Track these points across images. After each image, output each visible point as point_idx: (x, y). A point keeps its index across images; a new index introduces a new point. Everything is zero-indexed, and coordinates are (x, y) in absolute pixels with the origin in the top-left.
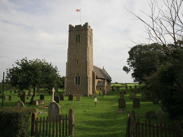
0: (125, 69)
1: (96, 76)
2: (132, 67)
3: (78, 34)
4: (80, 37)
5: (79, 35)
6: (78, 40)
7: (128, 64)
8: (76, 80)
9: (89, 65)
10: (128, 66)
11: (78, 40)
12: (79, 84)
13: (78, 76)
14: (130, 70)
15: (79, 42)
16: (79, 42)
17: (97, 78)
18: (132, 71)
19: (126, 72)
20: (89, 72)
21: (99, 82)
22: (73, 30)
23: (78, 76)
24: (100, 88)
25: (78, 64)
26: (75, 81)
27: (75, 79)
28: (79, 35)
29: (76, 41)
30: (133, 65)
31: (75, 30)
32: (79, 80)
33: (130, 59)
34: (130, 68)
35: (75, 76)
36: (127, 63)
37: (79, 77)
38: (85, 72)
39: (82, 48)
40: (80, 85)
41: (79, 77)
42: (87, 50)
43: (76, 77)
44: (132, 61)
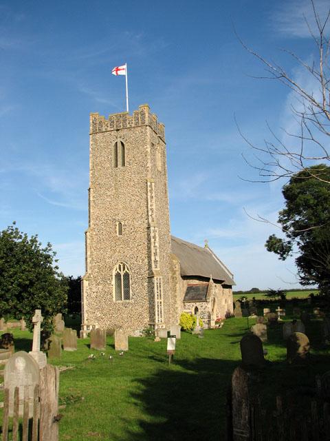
0: (274, 246)
1: (181, 268)
2: (298, 239)
3: (119, 140)
4: (126, 151)
5: (122, 143)
7: (285, 229)
8: (119, 286)
9: (154, 237)
10: (282, 236)
12: (127, 297)
13: (122, 273)
14: (289, 249)
15: (124, 164)
16: (124, 164)
17: (185, 277)
18: (296, 252)
19: (279, 256)
20: (158, 259)
21: (190, 289)
22: (104, 130)
23: (122, 273)
24: (196, 309)
25: (120, 232)
26: (114, 287)
27: (113, 282)
28: (122, 143)
29: (113, 161)
30: (299, 229)
31: (109, 129)
32: (127, 286)
33: (288, 213)
34: (289, 243)
35: (114, 273)
36: (280, 225)
37: (126, 275)
39: (132, 184)
43: (118, 276)
44: (297, 218)
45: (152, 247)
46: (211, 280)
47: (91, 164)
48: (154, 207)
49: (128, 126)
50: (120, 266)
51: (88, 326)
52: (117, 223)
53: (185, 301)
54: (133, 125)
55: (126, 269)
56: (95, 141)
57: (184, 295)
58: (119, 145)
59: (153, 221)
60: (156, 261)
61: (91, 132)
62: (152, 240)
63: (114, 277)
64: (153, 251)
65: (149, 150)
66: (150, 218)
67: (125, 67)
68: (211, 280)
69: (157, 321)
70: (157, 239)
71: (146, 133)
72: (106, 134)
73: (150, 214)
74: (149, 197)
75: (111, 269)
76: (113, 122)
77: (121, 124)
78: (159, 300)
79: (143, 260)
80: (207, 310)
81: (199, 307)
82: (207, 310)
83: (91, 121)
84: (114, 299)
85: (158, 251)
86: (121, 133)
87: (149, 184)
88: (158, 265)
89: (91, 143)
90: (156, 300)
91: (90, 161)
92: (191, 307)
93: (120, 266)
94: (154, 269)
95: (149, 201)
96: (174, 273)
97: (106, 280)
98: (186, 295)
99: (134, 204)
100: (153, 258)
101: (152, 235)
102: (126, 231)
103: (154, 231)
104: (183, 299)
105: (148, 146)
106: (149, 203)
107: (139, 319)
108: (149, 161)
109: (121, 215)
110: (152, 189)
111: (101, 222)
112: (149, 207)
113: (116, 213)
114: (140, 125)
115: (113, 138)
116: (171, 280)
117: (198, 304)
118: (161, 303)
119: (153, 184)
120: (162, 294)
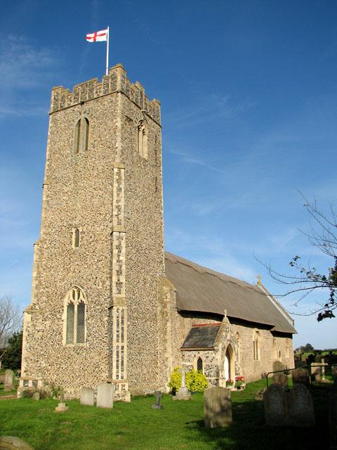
3: (83, 116)
6: (82, 142)
9: (119, 247)
11: (82, 142)
17: (184, 313)
20: (123, 279)
21: (195, 331)
24: (200, 361)
25: (77, 245)
26: (65, 323)
27: (65, 316)
29: (74, 146)
31: (72, 104)
32: (81, 322)
35: (66, 302)
37: (81, 306)
38: (104, 282)
40: (86, 345)
41: (81, 306)
42: (116, 177)
43: (71, 306)
45: (114, 261)
46: (226, 319)
47: (48, 153)
48: (122, 204)
49: (95, 96)
50: (74, 292)
51: (26, 381)
52: (74, 230)
53: (184, 348)
54: (101, 94)
55: (81, 297)
56: (55, 121)
57: (183, 340)
58: (83, 123)
59: (119, 223)
60: (119, 284)
61: (52, 111)
62: (115, 251)
63: (65, 308)
64: (115, 267)
65: (119, 124)
66: (115, 219)
67: (107, 31)
68: (226, 319)
69: (114, 377)
70: (123, 250)
71: (117, 101)
72: (69, 111)
73: (115, 213)
74: (115, 190)
75: (63, 297)
76: (78, 94)
77: (87, 96)
78: (120, 344)
79: (104, 282)
80: (214, 362)
81: (204, 359)
82: (214, 362)
83: (53, 98)
84: (64, 341)
85: (124, 267)
86: (86, 107)
87: (116, 170)
88: (123, 289)
89: (50, 125)
90: (115, 344)
91: (48, 149)
92: (192, 358)
93: (74, 292)
94: (115, 295)
95: (115, 194)
96: (165, 307)
97: (55, 313)
98: (187, 339)
99: (96, 201)
100: (115, 279)
101: (116, 243)
102: (84, 241)
103: (119, 238)
104: (181, 345)
105: (119, 119)
106: (115, 198)
107: (95, 374)
108: (119, 139)
109: (79, 217)
110: (120, 178)
111: (54, 230)
112: (115, 204)
113: (73, 215)
114: (110, 92)
115: (76, 114)
116: (159, 317)
117: (202, 354)
118: (123, 348)
119: (123, 171)
120: (125, 333)
